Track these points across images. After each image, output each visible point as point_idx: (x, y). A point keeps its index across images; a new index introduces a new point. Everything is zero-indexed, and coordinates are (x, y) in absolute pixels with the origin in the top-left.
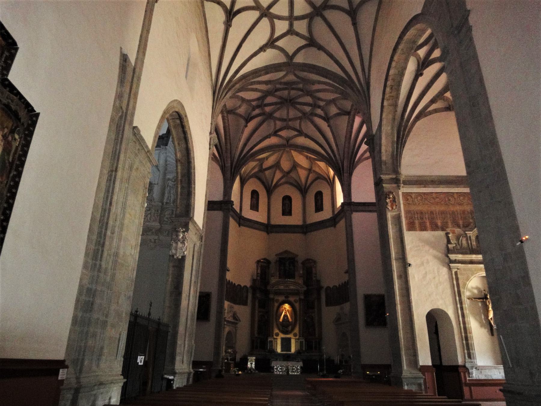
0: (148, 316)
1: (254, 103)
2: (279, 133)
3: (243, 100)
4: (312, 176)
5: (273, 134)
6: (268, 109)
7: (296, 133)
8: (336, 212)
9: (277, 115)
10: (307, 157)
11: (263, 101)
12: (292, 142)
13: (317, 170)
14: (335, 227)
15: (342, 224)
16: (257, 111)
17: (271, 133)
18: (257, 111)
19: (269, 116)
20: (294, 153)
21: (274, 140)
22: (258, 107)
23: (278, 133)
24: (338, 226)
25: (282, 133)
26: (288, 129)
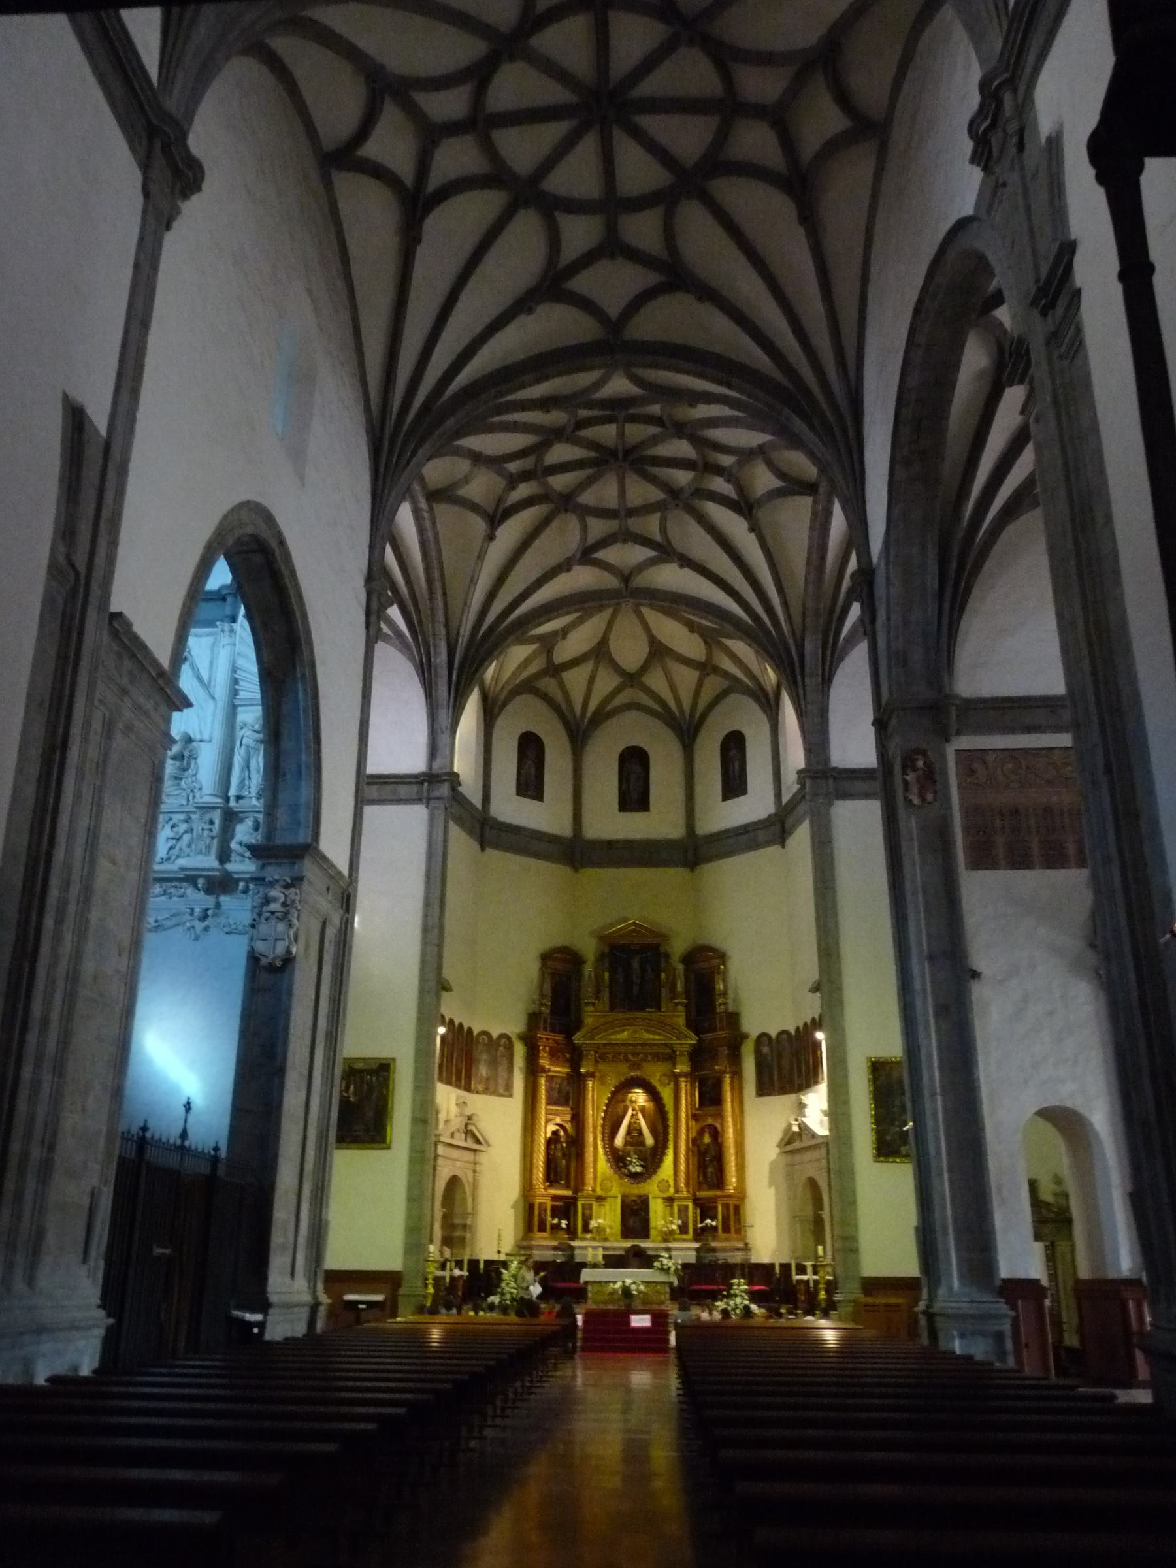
0: (179, 1142)
1: (513, 467)
2: (601, 555)
3: (477, 458)
4: (713, 685)
5: (578, 555)
6: (559, 482)
7: (649, 553)
8: (785, 799)
9: (587, 498)
10: (692, 627)
11: (540, 459)
12: (640, 581)
13: (727, 665)
14: (783, 846)
15: (802, 837)
16: (524, 490)
17: (574, 555)
18: (524, 490)
19: (565, 502)
20: (654, 618)
21: (582, 578)
22: (525, 476)
23: (596, 555)
24: (791, 841)
25: (610, 555)
26: (624, 541)
